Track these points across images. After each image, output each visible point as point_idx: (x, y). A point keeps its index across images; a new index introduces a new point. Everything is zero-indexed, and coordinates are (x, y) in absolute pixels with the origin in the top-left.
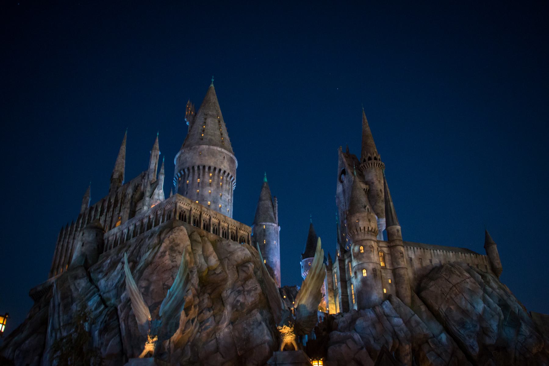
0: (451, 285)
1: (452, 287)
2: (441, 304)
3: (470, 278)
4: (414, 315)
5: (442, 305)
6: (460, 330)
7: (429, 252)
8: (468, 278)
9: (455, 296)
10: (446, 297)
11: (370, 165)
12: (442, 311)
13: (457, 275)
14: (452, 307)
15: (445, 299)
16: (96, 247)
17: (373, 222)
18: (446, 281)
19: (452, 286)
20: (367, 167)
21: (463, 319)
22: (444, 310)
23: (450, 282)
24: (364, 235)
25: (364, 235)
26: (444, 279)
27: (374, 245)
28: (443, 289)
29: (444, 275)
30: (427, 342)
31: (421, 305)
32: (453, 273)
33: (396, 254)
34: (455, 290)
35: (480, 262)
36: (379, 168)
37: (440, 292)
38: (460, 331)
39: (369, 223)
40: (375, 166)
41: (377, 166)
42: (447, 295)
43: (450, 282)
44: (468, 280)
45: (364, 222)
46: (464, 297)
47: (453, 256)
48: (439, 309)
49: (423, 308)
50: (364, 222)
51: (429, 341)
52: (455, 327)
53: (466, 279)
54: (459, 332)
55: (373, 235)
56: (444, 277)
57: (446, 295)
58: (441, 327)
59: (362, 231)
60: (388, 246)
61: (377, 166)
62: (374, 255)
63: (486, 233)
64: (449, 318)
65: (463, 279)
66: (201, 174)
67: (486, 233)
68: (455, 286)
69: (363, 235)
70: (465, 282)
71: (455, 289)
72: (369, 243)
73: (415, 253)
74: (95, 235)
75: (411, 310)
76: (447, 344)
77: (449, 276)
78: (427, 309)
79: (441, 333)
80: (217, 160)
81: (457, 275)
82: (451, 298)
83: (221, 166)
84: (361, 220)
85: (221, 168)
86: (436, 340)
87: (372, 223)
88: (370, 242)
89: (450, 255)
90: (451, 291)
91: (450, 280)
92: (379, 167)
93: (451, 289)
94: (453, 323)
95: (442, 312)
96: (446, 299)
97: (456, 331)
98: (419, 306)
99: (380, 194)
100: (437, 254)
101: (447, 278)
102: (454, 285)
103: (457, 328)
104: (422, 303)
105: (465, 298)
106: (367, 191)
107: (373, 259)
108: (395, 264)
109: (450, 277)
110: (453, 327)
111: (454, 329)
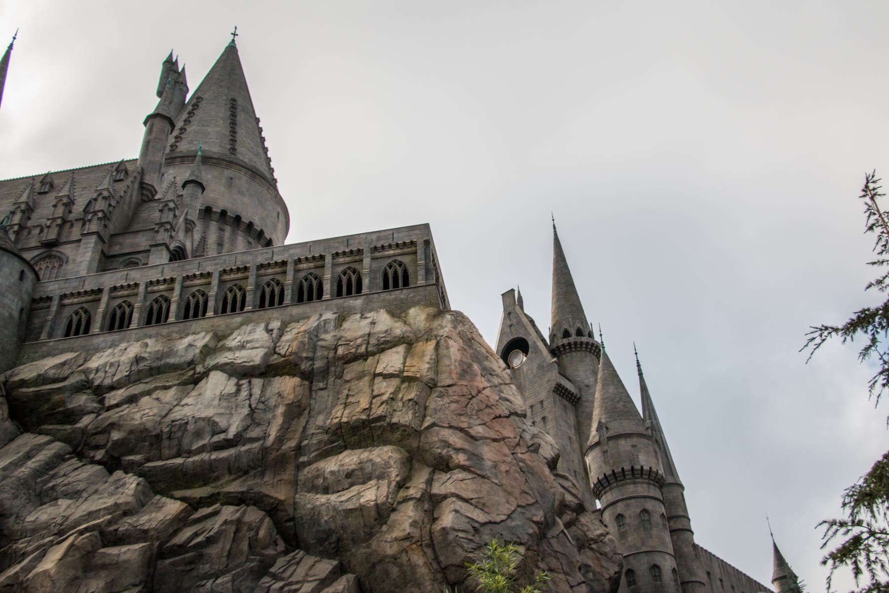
11: (584, 346)
16: (16, 314)
25: (649, 488)
33: (686, 550)
59: (644, 476)
74: (17, 276)
83: (272, 233)
84: (642, 450)
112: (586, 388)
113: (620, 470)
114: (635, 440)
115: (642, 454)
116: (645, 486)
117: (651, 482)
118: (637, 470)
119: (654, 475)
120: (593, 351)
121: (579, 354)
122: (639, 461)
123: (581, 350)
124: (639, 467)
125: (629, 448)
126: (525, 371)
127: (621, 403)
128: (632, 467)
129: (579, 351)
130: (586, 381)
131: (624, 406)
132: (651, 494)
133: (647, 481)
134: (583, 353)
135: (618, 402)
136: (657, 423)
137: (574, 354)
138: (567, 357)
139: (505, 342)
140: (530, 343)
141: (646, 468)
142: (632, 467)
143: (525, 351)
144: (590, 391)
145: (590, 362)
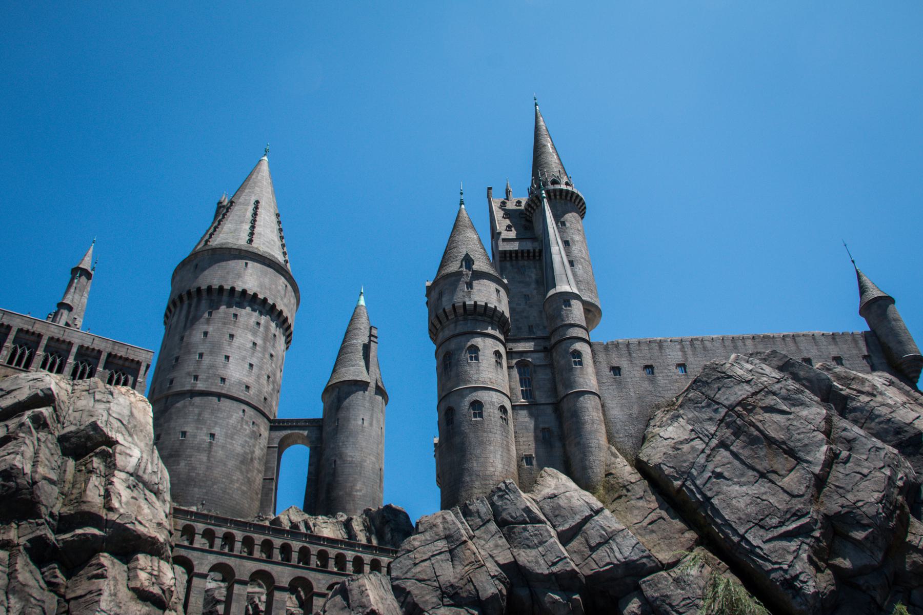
0: (723, 411)
4: (598, 512)
12: (692, 487)
20: (536, 204)
24: (456, 326)
28: (697, 427)
36: (563, 202)
40: (553, 197)
41: (558, 197)
43: (718, 403)
48: (683, 485)
49: (641, 487)
55: (484, 321)
59: (450, 318)
61: (558, 197)
66: (194, 305)
69: (452, 326)
73: (630, 354)
80: (228, 273)
85: (235, 285)
92: (563, 197)
93: (721, 421)
95: (691, 491)
97: (736, 539)
104: (635, 477)
106: (537, 254)
107: (475, 377)
108: (560, 388)
119: (461, 311)
132: (457, 331)
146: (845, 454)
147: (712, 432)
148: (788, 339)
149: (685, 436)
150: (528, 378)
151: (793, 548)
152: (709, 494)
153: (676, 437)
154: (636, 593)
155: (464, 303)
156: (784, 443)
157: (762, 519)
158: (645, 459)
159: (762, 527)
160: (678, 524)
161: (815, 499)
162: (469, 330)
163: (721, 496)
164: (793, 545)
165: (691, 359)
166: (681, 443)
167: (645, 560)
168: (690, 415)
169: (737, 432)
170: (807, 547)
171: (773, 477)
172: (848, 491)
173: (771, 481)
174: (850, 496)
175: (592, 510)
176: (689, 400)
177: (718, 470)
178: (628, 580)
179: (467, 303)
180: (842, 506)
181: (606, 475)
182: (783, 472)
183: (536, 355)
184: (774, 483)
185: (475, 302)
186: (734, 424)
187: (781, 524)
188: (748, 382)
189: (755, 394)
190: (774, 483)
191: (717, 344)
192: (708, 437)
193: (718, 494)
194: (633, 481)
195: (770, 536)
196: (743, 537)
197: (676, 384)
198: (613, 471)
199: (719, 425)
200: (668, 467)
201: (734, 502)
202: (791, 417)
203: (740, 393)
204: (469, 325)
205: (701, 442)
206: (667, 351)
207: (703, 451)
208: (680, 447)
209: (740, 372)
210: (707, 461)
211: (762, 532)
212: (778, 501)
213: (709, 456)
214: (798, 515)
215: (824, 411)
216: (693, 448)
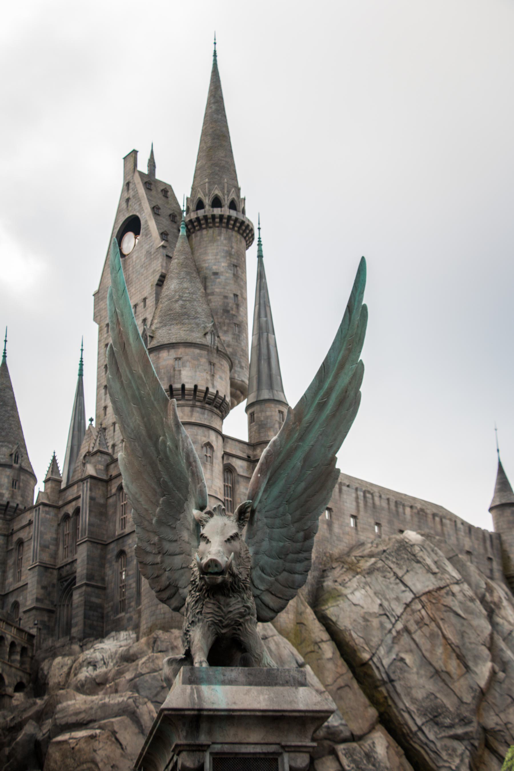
0: (408, 597)
1: (411, 602)
2: (379, 645)
3: (462, 583)
5: (381, 648)
6: (424, 728)
7: (354, 495)
8: (457, 583)
9: (416, 627)
10: (394, 625)
12: (379, 665)
13: (429, 570)
14: (408, 659)
15: (390, 631)
17: (221, 378)
18: (398, 581)
19: (413, 599)
21: (436, 697)
22: (386, 662)
23: (406, 585)
24: (192, 411)
25: (192, 411)
26: (392, 574)
27: (214, 444)
28: (386, 604)
29: (392, 566)
30: (333, 752)
31: (322, 641)
32: (418, 562)
34: (419, 611)
35: (476, 546)
37: (376, 609)
38: (426, 731)
39: (209, 378)
42: (396, 621)
43: (406, 585)
44: (456, 589)
45: (196, 371)
46: (442, 633)
47: (412, 516)
48: (371, 659)
50: (196, 371)
51: (341, 748)
52: (413, 719)
53: (451, 584)
54: (423, 732)
55: (218, 415)
56: (391, 568)
57: (393, 620)
58: (372, 712)
59: (187, 397)
60: (249, 457)
62: (212, 471)
63: (501, 470)
64: (399, 689)
65: (442, 584)
67: (501, 470)
68: (417, 597)
70: (447, 594)
71: (419, 606)
72: (205, 436)
75: (295, 652)
76: (388, 765)
77: (405, 567)
78: (338, 654)
79: (372, 729)
81: (429, 570)
82: (406, 629)
84: (188, 364)
86: (358, 748)
87: (219, 380)
88: (206, 433)
89: (404, 513)
90: (408, 609)
91: (407, 579)
93: (408, 605)
94: (407, 705)
95: (378, 668)
96: (394, 633)
97: (414, 729)
98: (316, 643)
99: (232, 309)
100: (374, 504)
101: (400, 574)
102: (417, 595)
103: (419, 722)
104: (325, 636)
105: (444, 636)
109: (408, 571)
110: (406, 715)
111: (410, 722)
112: (212, 277)
113: (192, 387)
114: (181, 351)
115: (187, 369)
116: (187, 409)
117: (198, 404)
118: (177, 390)
120: (231, 226)
121: (211, 231)
122: (180, 378)
123: (214, 226)
124: (179, 386)
125: (171, 362)
126: (134, 260)
127: (181, 302)
128: (171, 387)
129: (211, 227)
130: (214, 267)
131: (183, 307)
132: (193, 420)
133: (191, 403)
134: (217, 230)
135: (177, 301)
136: (267, 322)
137: (204, 232)
138: (196, 236)
139: (120, 222)
140: (142, 222)
141: (189, 386)
142: (171, 387)
143: (137, 233)
144: (218, 280)
145: (225, 242)
146: (501, 675)
147: (399, 614)
148: (437, 519)
149: (376, 609)
150: (230, 487)
151: (459, 752)
152: (393, 676)
153: (365, 606)
154: (331, 757)
155: (207, 389)
156: (458, 647)
157: (435, 717)
158: (334, 619)
159: (437, 724)
160: (363, 699)
161: (477, 710)
162: (206, 423)
163: (402, 683)
164: (460, 747)
165: (362, 513)
166: (370, 614)
167: (341, 728)
168: (378, 588)
169: (420, 623)
170: (468, 753)
171: (445, 676)
172: (502, 711)
173: (443, 681)
174: (502, 716)
175: (297, 662)
176: (378, 569)
177: (403, 655)
178: (327, 743)
179: (211, 390)
180: (497, 724)
181: (298, 623)
182: (455, 677)
183: (244, 464)
184: (446, 684)
185: (217, 392)
186: (418, 613)
187: (451, 726)
188: (434, 574)
189: (440, 589)
190: (446, 684)
191: (384, 504)
192: (395, 617)
193: (399, 679)
194: (324, 639)
195: (443, 734)
196: (420, 729)
197: (347, 537)
198: (305, 622)
199: (405, 609)
200: (358, 636)
201: (414, 692)
202: (465, 623)
203: (427, 583)
204: (206, 416)
205: (388, 621)
206: (345, 496)
207: (390, 631)
208: (370, 619)
209: (429, 561)
210: (393, 642)
211: (436, 729)
212: (449, 703)
213: (394, 638)
214: (465, 721)
215: (490, 627)
216: (382, 625)
